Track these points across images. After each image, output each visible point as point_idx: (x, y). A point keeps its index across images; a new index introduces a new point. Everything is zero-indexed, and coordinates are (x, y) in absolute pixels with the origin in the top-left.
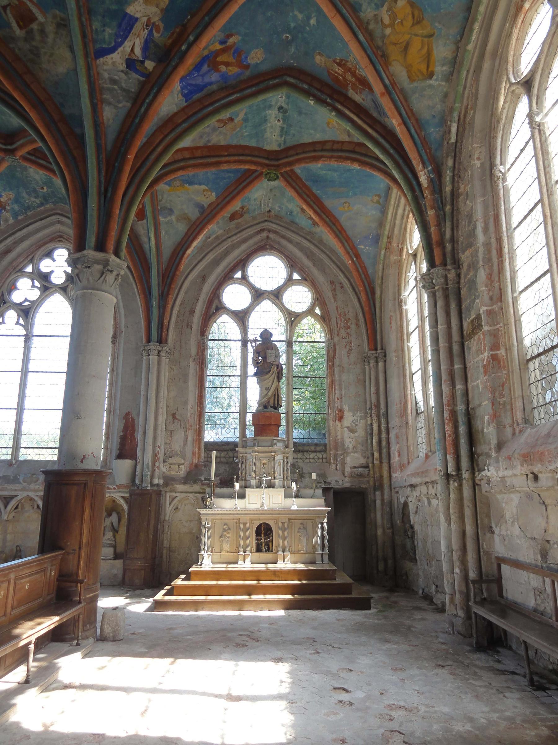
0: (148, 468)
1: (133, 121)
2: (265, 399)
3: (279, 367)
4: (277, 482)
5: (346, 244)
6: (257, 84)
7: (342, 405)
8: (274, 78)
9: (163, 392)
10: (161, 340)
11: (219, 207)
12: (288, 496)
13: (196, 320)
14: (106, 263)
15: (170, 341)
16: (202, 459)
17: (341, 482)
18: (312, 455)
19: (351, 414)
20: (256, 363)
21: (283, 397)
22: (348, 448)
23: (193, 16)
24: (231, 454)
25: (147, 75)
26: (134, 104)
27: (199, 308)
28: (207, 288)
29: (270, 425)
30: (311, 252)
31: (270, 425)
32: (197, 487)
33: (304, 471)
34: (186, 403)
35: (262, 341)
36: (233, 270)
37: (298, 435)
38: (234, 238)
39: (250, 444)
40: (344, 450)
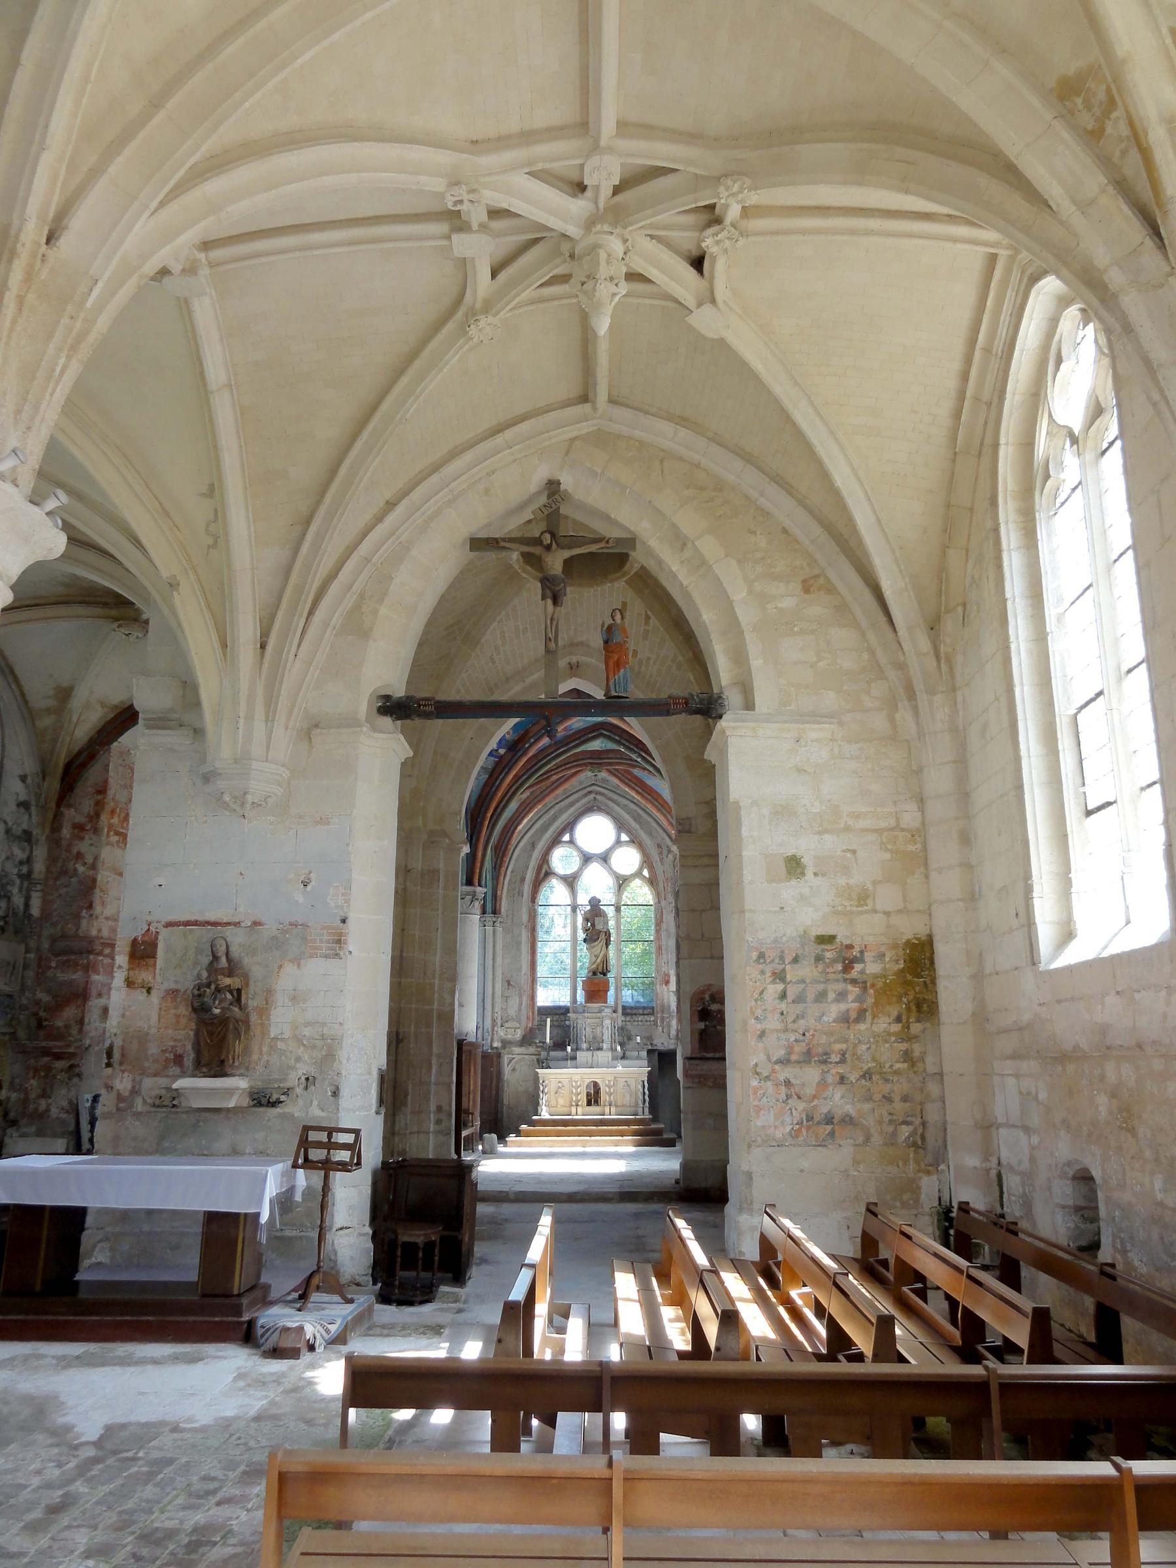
2: (594, 966)
3: (608, 935)
4: (605, 1046)
8: (593, 731)
9: (499, 960)
12: (615, 1058)
13: (527, 888)
14: (474, 894)
15: (503, 910)
20: (586, 930)
25: (501, 757)
26: (491, 775)
27: (530, 876)
30: (638, 814)
32: (532, 1050)
33: (633, 1033)
34: (519, 970)
36: (561, 833)
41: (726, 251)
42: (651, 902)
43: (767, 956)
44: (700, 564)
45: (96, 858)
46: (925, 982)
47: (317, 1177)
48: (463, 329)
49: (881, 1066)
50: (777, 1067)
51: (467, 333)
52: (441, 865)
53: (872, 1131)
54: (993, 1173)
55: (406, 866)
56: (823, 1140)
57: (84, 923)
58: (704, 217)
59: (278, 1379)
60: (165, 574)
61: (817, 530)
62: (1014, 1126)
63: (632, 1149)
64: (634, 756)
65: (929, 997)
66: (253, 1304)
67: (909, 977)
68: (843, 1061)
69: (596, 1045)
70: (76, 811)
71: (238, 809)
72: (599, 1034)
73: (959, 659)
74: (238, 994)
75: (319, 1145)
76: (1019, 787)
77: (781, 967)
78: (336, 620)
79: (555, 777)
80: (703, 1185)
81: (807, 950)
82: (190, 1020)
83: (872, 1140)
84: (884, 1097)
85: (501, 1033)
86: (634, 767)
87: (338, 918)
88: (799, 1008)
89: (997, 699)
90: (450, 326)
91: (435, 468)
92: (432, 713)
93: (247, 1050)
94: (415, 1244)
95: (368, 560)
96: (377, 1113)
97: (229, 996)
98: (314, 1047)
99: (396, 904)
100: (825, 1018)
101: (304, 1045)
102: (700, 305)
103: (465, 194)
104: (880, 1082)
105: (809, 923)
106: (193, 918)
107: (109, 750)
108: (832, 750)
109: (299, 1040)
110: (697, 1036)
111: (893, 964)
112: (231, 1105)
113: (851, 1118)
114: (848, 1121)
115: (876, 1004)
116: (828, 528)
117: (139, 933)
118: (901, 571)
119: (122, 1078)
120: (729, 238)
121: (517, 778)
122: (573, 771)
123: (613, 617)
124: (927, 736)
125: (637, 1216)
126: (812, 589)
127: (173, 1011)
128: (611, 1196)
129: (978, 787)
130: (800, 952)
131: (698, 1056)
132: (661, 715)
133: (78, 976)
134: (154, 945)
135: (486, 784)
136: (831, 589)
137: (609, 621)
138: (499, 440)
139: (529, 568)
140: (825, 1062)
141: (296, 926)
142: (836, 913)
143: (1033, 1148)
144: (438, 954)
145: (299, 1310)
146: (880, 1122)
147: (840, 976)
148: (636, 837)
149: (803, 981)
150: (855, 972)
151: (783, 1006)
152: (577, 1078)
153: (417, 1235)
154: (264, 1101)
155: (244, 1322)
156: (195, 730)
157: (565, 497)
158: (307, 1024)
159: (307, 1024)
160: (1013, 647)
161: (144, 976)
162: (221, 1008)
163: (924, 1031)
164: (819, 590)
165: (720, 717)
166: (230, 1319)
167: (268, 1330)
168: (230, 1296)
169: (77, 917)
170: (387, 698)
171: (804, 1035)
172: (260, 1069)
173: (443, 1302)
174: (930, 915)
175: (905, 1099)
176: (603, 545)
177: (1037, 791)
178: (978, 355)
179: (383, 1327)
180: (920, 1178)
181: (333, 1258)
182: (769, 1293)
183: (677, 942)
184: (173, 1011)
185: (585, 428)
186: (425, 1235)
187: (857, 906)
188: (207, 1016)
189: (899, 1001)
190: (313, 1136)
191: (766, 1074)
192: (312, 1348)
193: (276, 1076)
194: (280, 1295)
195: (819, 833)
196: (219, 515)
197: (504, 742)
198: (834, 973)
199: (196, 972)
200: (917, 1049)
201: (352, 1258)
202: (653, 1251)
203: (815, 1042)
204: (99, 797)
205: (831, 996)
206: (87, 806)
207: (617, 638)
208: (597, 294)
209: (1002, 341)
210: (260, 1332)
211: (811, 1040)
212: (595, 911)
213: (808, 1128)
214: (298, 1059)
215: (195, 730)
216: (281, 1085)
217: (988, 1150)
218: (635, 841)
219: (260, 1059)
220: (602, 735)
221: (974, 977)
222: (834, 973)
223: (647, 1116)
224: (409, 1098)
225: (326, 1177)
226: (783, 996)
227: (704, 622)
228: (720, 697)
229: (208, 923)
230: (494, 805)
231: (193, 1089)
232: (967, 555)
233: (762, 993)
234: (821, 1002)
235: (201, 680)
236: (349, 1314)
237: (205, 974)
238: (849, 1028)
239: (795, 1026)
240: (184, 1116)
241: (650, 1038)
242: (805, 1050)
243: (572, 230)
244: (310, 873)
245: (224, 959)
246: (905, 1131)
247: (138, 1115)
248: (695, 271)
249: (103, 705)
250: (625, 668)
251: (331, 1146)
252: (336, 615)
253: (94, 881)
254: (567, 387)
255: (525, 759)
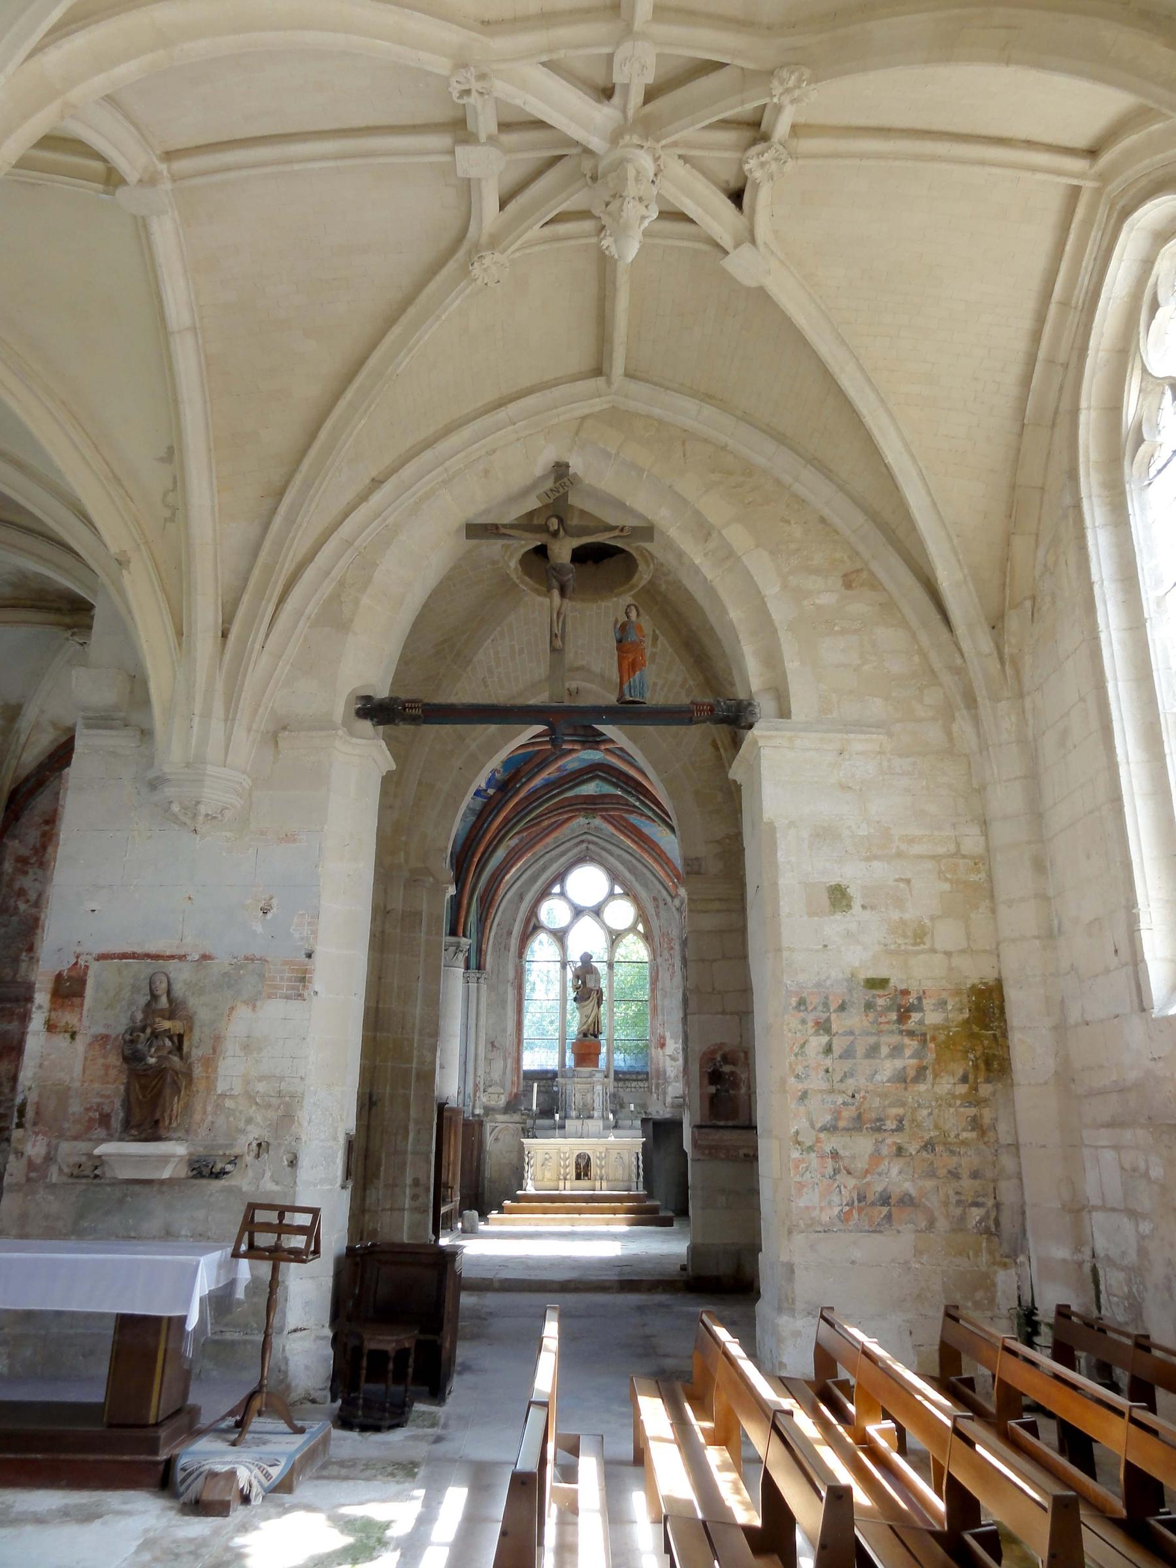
0: (469, 1097)
1: (477, 833)
2: (585, 1027)
3: (600, 993)
4: (596, 1114)
5: (666, 867)
6: (574, 779)
7: (664, 1032)
8: (588, 773)
10: (480, 967)
11: (538, 838)
12: (606, 1128)
13: (514, 942)
14: (458, 946)
15: (488, 966)
16: (521, 1089)
17: (661, 1112)
18: (634, 1084)
19: (672, 1041)
20: (576, 988)
21: (604, 1021)
22: (670, 1077)
23: (525, 764)
24: (550, 1082)
25: (490, 798)
26: (478, 818)
27: (517, 929)
28: (525, 906)
29: (590, 1054)
30: (633, 865)
31: (590, 1054)
32: (517, 1117)
33: (625, 1101)
34: (504, 1030)
35: (582, 961)
37: (621, 1060)
38: (553, 852)
39: (570, 1074)
40: (665, 1079)
41: (771, 177)
42: (646, 959)
43: (808, 1002)
44: (728, 556)
45: (40, 896)
46: (994, 1035)
47: (265, 1268)
48: (465, 271)
49: (945, 1134)
50: (822, 1135)
51: (470, 272)
52: (425, 907)
53: (937, 1214)
54: (1087, 1268)
55: (385, 907)
56: (878, 1224)
57: (24, 966)
58: (747, 134)
59: (197, 1548)
60: (114, 549)
61: (860, 518)
62: (1113, 1210)
63: (625, 1228)
64: (632, 800)
65: (999, 1052)
66: (172, 1438)
67: (976, 1029)
68: (900, 1129)
69: (586, 1114)
70: (20, 842)
71: (188, 822)
72: (589, 1101)
73: (1028, 660)
74: (179, 1041)
75: (267, 1227)
76: (1116, 800)
77: (825, 1016)
78: (312, 609)
79: (546, 823)
80: (715, 1273)
81: (855, 995)
82: (120, 1072)
83: (937, 1224)
84: (950, 1172)
85: (484, 1099)
86: (632, 812)
87: (303, 952)
88: (847, 1065)
89: (1082, 699)
90: (451, 266)
91: (429, 444)
92: (420, 717)
93: (188, 1108)
94: (384, 1353)
95: (349, 543)
96: (343, 1187)
97: (168, 1043)
98: (269, 1106)
99: (372, 947)
100: (878, 1077)
101: (257, 1104)
102: (737, 245)
103: (473, 80)
104: (944, 1154)
105: (857, 964)
106: (129, 949)
107: (60, 777)
108: (880, 764)
109: (251, 1098)
110: (707, 1104)
111: (957, 1014)
112: (166, 1174)
113: (911, 1198)
114: (907, 1201)
115: (938, 1060)
116: (873, 516)
117: (64, 967)
118: (959, 561)
119: (35, 1141)
120: (776, 159)
121: (507, 820)
122: (565, 816)
123: (627, 614)
124: (990, 749)
125: (640, 1309)
126: (854, 585)
127: (101, 1061)
128: (608, 1284)
129: (1055, 804)
130: (847, 999)
131: (709, 1123)
132: (681, 723)
133: (13, 1026)
134: (82, 982)
135: (474, 826)
136: (874, 584)
137: (622, 618)
138: (502, 414)
139: (527, 579)
140: (879, 1130)
141: (252, 960)
142: (890, 953)
143: (1142, 1237)
144: (418, 1008)
145: (234, 1444)
146: (946, 1204)
147: (895, 1027)
148: (630, 889)
149: (852, 1033)
150: (911, 1024)
151: (828, 1062)
152: (566, 1149)
153: (387, 1341)
154: (206, 1171)
155: (157, 1463)
156: (143, 732)
157: (574, 481)
158: (261, 1079)
159: (261, 1079)
160: (1103, 636)
161: (67, 1018)
162: (159, 1057)
163: (994, 1094)
164: (862, 585)
165: (751, 726)
166: (142, 1457)
167: (190, 1474)
168: (145, 1426)
169: (16, 960)
170: (368, 698)
171: (853, 1096)
172: (202, 1132)
173: (418, 1426)
174: (998, 956)
175: (975, 1175)
176: (616, 533)
177: (1139, 803)
178: (1053, 309)
179: (342, 1464)
180: (995, 1273)
181: (283, 1368)
182: (840, 1429)
183: (684, 995)
184: (101, 1061)
185: (599, 404)
186: (397, 1341)
187: (915, 944)
188: (140, 1066)
189: (966, 1058)
190: (261, 1216)
191: (808, 1143)
192: (246, 1499)
193: (221, 1141)
194: (212, 1421)
195: (868, 859)
196: (178, 483)
197: (493, 782)
198: (888, 1023)
199: (129, 1013)
200: (987, 1115)
201: (307, 1368)
202: (666, 1356)
203: (866, 1106)
204: (47, 828)
205: (885, 1050)
206: (33, 836)
207: (633, 637)
208: (624, 214)
209: (1084, 291)
210: (180, 1476)
211: (862, 1103)
212: (586, 970)
213: (860, 1210)
214: (249, 1121)
215: (143, 732)
216: (227, 1152)
217: (1079, 1241)
218: (629, 894)
219: (203, 1120)
220: (597, 777)
221: (1055, 1028)
222: (888, 1023)
223: (642, 1192)
224: (382, 1169)
225: (275, 1270)
226: (828, 1050)
227: (731, 621)
228: (750, 704)
229: (148, 956)
230: (481, 849)
231: (121, 1155)
232: (1037, 541)
233: (803, 1046)
234: (873, 1058)
235: (151, 672)
236: (297, 1451)
237: (139, 1016)
238: (906, 1089)
239: (843, 1086)
240: (108, 1189)
241: (643, 1106)
242: (855, 1115)
243: (596, 143)
244: (271, 899)
245: (164, 1000)
246: (976, 1214)
247: (52, 1187)
248: (733, 206)
249: (54, 725)
250: (641, 670)
251: (282, 1229)
252: (311, 604)
253: (37, 920)
254: (578, 357)
255: (516, 800)
